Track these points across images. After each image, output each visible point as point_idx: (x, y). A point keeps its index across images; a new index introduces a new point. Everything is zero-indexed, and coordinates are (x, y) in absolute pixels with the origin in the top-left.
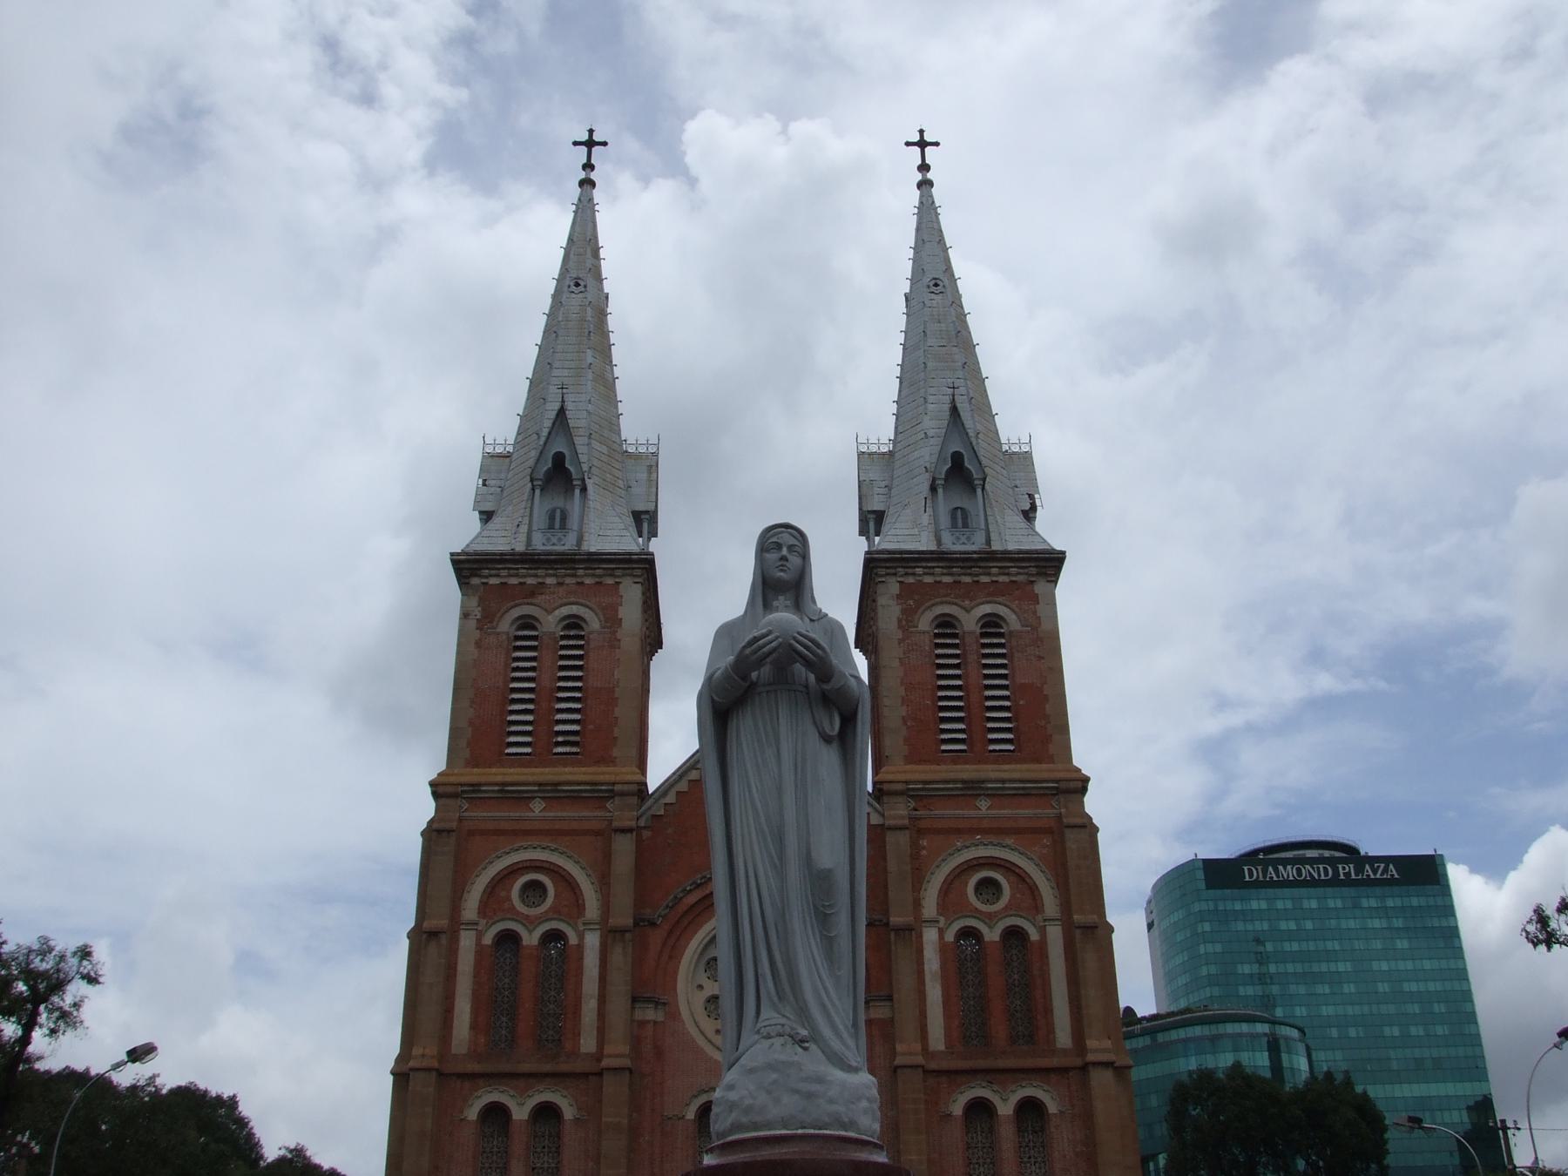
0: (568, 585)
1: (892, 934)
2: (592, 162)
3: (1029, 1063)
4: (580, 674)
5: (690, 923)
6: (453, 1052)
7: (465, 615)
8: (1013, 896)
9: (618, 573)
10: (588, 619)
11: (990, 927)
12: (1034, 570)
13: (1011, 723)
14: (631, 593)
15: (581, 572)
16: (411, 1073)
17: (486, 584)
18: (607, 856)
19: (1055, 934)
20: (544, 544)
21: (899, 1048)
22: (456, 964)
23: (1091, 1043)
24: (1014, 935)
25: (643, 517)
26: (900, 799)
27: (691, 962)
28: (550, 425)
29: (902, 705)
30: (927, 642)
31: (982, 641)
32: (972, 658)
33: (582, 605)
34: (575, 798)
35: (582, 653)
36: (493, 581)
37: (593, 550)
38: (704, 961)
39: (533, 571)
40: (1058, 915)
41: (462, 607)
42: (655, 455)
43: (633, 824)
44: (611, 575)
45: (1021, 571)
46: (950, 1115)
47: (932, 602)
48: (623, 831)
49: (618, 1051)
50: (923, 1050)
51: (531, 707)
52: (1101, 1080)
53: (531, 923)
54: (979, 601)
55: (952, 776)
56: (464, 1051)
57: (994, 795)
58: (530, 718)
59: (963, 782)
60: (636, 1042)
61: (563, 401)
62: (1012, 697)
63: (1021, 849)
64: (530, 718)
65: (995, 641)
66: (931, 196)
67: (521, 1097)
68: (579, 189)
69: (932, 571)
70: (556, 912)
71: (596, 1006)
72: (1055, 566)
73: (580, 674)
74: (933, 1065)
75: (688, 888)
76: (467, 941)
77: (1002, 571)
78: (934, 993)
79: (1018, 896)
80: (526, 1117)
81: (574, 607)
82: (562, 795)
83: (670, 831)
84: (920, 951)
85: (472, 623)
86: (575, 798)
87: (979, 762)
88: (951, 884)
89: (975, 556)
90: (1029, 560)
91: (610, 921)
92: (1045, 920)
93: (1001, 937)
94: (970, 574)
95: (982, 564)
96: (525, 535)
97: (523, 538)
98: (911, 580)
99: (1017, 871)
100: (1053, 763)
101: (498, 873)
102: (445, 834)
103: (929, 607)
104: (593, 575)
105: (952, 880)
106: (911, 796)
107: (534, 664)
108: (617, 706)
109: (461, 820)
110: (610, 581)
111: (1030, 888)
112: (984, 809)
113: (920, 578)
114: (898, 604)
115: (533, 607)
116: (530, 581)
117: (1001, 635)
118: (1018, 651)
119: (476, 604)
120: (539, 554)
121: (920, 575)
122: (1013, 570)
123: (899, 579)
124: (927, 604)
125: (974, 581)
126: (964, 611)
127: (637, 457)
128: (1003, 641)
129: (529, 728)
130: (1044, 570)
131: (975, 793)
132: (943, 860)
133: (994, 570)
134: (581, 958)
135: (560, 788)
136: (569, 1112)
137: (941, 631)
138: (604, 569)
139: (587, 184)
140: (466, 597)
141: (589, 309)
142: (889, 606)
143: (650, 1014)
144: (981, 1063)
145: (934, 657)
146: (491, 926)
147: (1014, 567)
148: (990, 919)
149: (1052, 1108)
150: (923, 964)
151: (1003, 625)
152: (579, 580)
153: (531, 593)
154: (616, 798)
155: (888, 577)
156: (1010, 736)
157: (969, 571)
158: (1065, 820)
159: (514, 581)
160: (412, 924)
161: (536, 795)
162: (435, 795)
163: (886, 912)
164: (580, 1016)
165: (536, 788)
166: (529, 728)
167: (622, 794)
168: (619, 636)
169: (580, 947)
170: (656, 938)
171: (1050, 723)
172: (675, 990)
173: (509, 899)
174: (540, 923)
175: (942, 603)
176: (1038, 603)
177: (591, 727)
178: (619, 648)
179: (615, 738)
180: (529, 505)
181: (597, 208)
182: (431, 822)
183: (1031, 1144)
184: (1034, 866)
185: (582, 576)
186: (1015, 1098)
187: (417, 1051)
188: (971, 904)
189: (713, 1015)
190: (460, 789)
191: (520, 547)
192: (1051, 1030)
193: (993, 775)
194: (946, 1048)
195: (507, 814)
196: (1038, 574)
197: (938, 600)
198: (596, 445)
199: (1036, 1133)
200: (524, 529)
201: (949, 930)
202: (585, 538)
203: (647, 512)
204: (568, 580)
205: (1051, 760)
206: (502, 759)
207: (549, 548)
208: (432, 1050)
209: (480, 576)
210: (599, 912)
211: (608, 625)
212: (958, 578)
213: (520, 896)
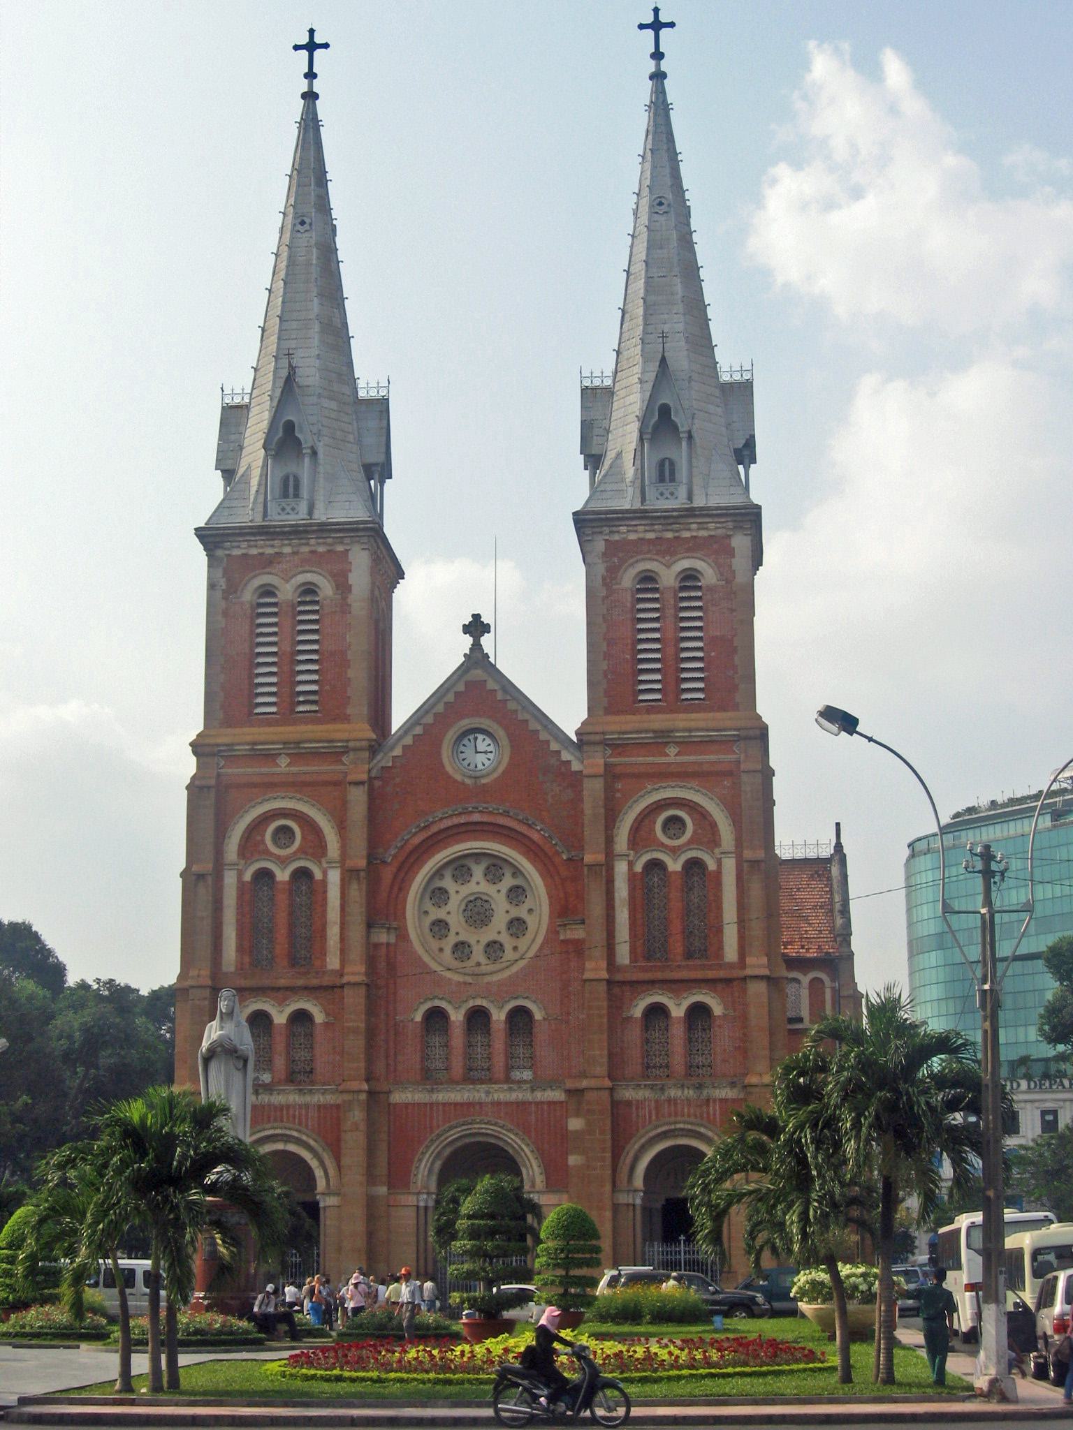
0: (302, 553)
1: (586, 869)
2: (314, 71)
3: (699, 975)
4: (316, 637)
5: (416, 860)
6: (225, 969)
7: (212, 586)
8: (695, 832)
9: (347, 541)
10: (321, 586)
11: (675, 860)
12: (730, 525)
13: (703, 673)
14: (360, 560)
15: (313, 542)
16: (190, 991)
17: (229, 555)
18: (344, 803)
19: (729, 865)
20: (279, 514)
21: (588, 965)
22: (222, 898)
23: (749, 960)
24: (694, 866)
25: (373, 468)
26: (600, 748)
27: (415, 901)
28: (282, 385)
29: (604, 659)
30: (629, 599)
31: (680, 595)
32: (670, 612)
33: (314, 572)
34: (316, 755)
35: (317, 617)
36: (237, 552)
37: (323, 519)
38: (429, 890)
39: (272, 542)
40: (733, 849)
41: (208, 578)
42: (388, 399)
43: (365, 777)
44: (342, 543)
45: (718, 525)
46: (631, 1017)
47: (634, 559)
48: (357, 784)
49: (357, 972)
50: (608, 965)
51: (274, 669)
52: (758, 990)
53: (283, 862)
54: (679, 556)
55: (645, 726)
56: (232, 969)
57: (682, 743)
58: (274, 680)
59: (654, 731)
60: (371, 961)
61: (290, 365)
62: (705, 649)
63: (704, 791)
64: (274, 680)
65: (693, 594)
66: (664, 92)
67: (280, 1005)
68: (303, 101)
69: (635, 528)
70: (302, 851)
71: (339, 931)
72: (750, 521)
73: (316, 637)
74: (618, 977)
75: (414, 830)
76: (230, 879)
77: (701, 526)
78: (622, 916)
79: (700, 831)
80: (285, 1022)
81: (309, 575)
82: (303, 751)
83: (398, 780)
84: (610, 881)
85: (219, 594)
86: (316, 755)
87: (671, 711)
88: (641, 821)
89: (675, 514)
90: (726, 515)
91: (348, 861)
92: (722, 853)
93: (684, 867)
94: (671, 530)
95: (682, 520)
96: (262, 505)
97: (260, 508)
98: (616, 537)
99: (700, 809)
100: (738, 710)
101: (253, 820)
102: (205, 790)
103: (632, 565)
104: (324, 544)
105: (643, 819)
106: (607, 745)
107: (275, 629)
108: (349, 667)
109: (219, 775)
110: (340, 548)
111: (711, 824)
112: (672, 754)
113: (625, 536)
114: (603, 562)
115: (270, 576)
116: (270, 551)
117: (700, 588)
118: (713, 605)
119: (221, 576)
120: (275, 527)
121: (624, 533)
122: (712, 526)
123: (607, 538)
124: (631, 561)
125: (675, 537)
126: (664, 567)
127: (370, 402)
128: (700, 594)
129: (274, 689)
130: (741, 524)
131: (665, 740)
132: (635, 802)
133: (694, 526)
134: (325, 892)
135: (302, 745)
136: (319, 1017)
137: (643, 586)
138: (334, 538)
139: (310, 97)
140: (211, 569)
141: (314, 250)
142: (595, 564)
143: (382, 937)
144: (659, 975)
145: (635, 611)
146: (249, 865)
147: (712, 522)
148: (674, 851)
149: (717, 1010)
150: (613, 892)
151: (700, 577)
152: (313, 548)
153: (267, 562)
154: (352, 755)
155: (595, 536)
156: (701, 685)
157: (669, 527)
158: (742, 767)
159: (254, 551)
160: (184, 866)
161: (281, 751)
162: (195, 753)
163: (581, 848)
164: (326, 939)
165: (281, 746)
166: (274, 689)
167: (355, 749)
168: (349, 601)
169: (324, 882)
170: (387, 874)
171: (737, 673)
172: (404, 913)
173: (263, 841)
174: (290, 863)
175: (643, 560)
176: (734, 557)
177: (327, 687)
178: (350, 613)
179: (349, 698)
180: (265, 473)
181: (320, 123)
182: (193, 778)
183: (700, 1040)
184: (714, 805)
185: (314, 545)
186: (686, 1004)
187: (193, 973)
188: (658, 839)
189: (437, 937)
190: (216, 749)
191: (259, 521)
192: (720, 947)
193: (681, 725)
194: (630, 962)
195: (257, 770)
196: (735, 527)
197: (641, 557)
198: (326, 403)
199: (704, 1030)
200: (261, 499)
201: (637, 864)
202: (317, 506)
203: (376, 464)
204: (305, 549)
205: (736, 707)
206: (251, 717)
207: (284, 517)
208: (206, 972)
209: (222, 548)
210: (339, 852)
211: (340, 592)
212: (659, 535)
213: (272, 841)
